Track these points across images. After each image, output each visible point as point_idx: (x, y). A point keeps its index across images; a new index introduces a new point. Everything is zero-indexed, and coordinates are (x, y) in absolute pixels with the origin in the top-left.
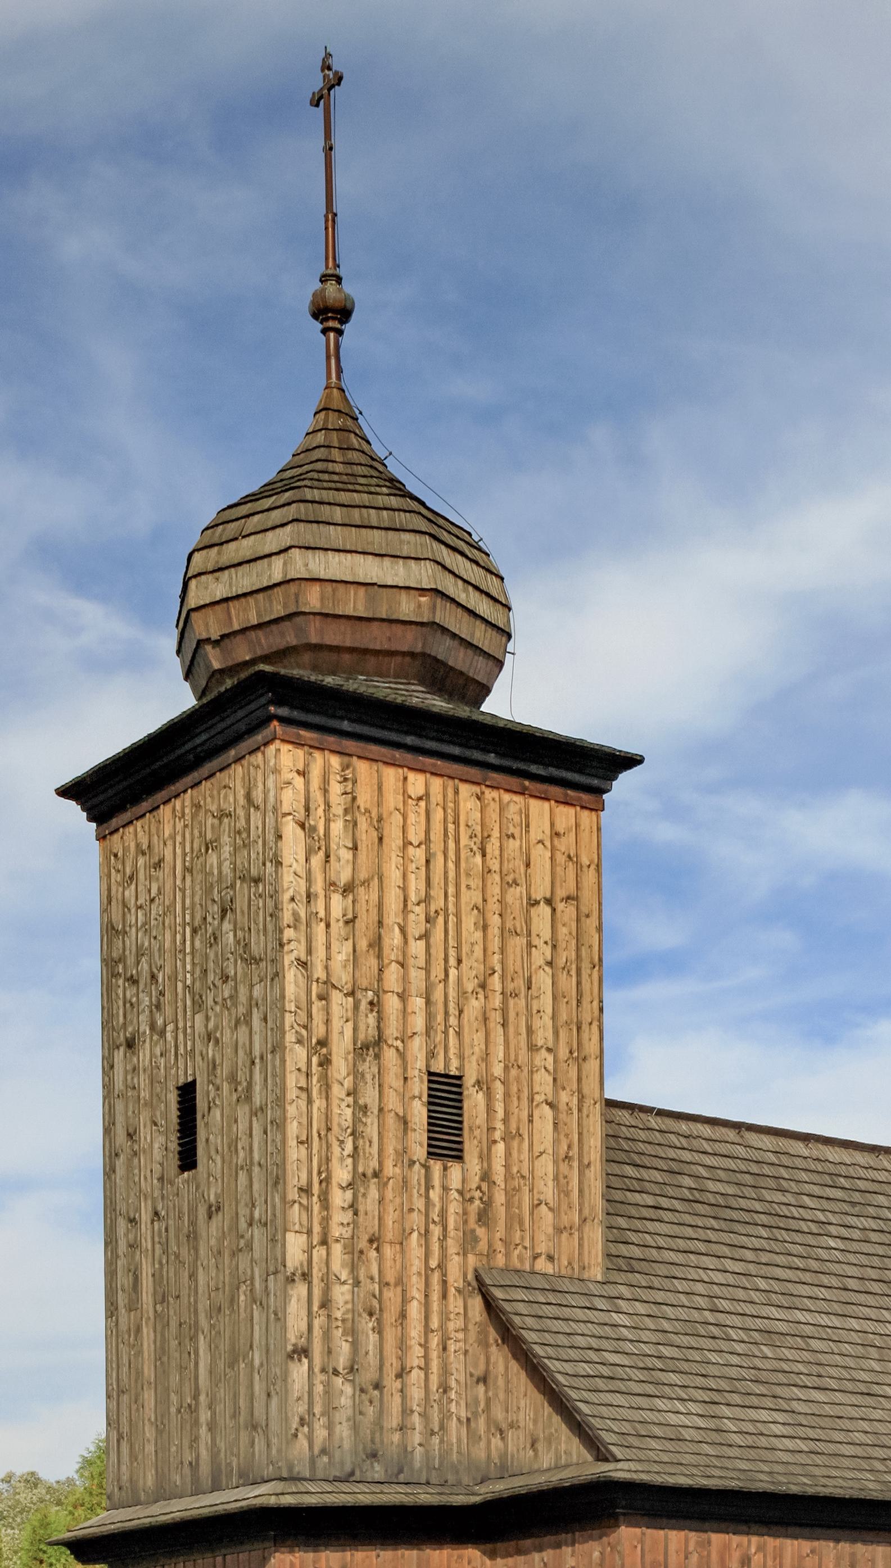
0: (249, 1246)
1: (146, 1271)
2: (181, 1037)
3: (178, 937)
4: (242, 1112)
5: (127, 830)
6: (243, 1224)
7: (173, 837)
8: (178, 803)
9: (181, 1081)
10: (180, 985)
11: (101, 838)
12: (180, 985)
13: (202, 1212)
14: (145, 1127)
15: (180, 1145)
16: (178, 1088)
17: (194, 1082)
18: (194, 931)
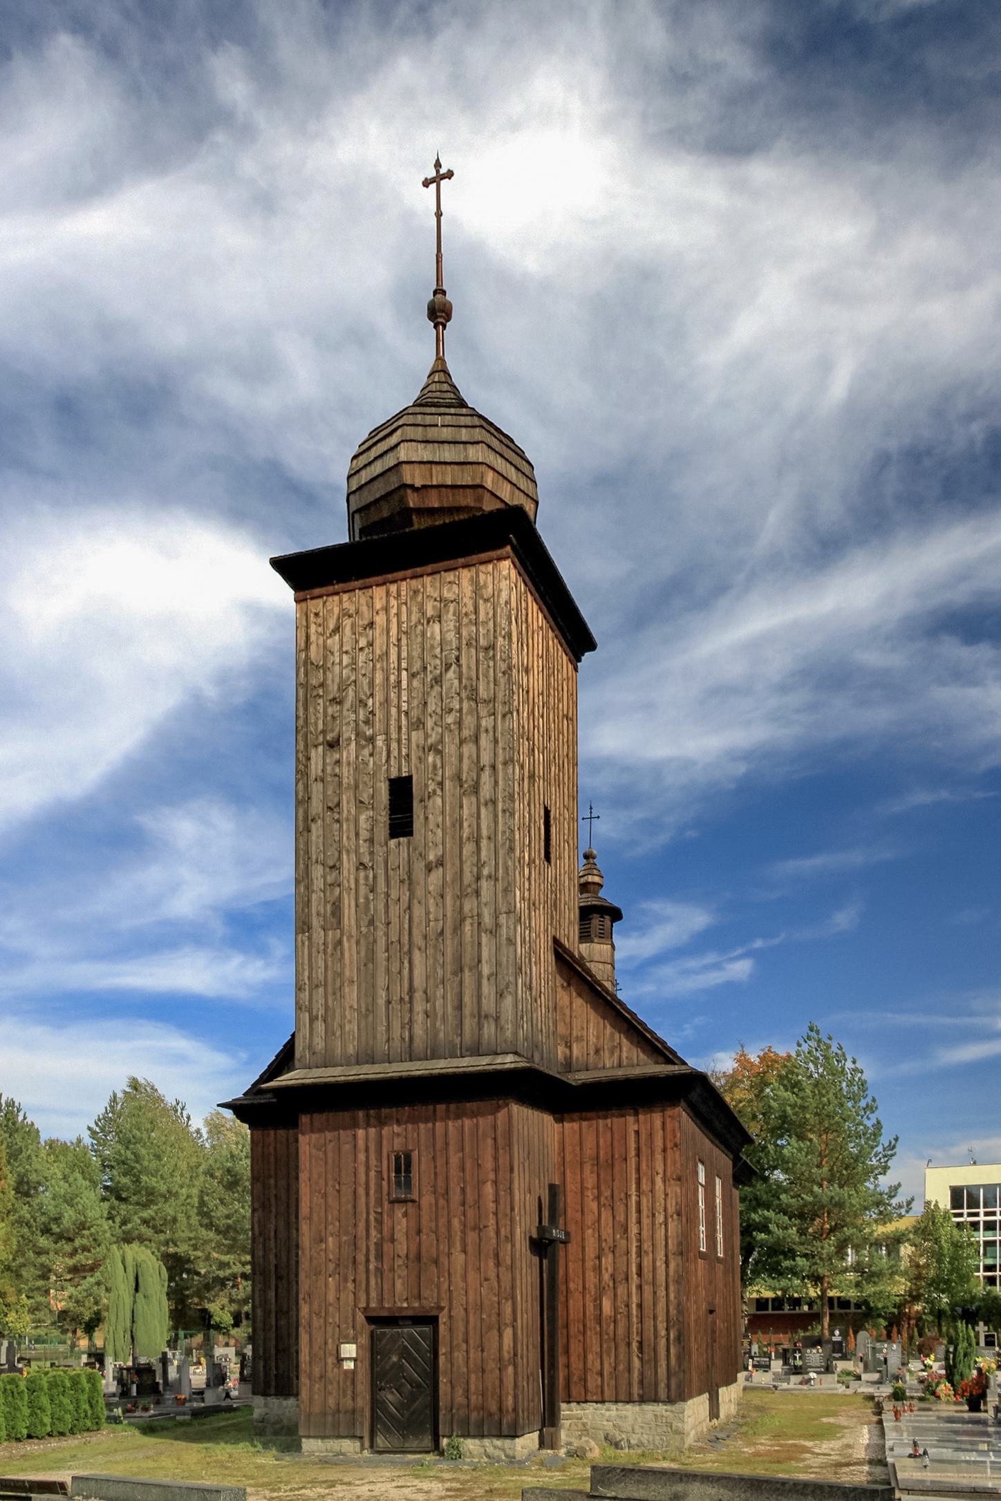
0: (477, 893)
1: (348, 904)
2: (394, 745)
3: (393, 678)
4: (468, 804)
5: (330, 599)
6: (468, 877)
7: (386, 609)
8: (393, 588)
9: (394, 774)
10: (394, 711)
11: (297, 601)
12: (394, 711)
13: (419, 866)
14: (348, 803)
15: (390, 819)
16: (391, 781)
17: (410, 778)
18: (413, 676)
